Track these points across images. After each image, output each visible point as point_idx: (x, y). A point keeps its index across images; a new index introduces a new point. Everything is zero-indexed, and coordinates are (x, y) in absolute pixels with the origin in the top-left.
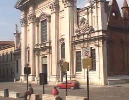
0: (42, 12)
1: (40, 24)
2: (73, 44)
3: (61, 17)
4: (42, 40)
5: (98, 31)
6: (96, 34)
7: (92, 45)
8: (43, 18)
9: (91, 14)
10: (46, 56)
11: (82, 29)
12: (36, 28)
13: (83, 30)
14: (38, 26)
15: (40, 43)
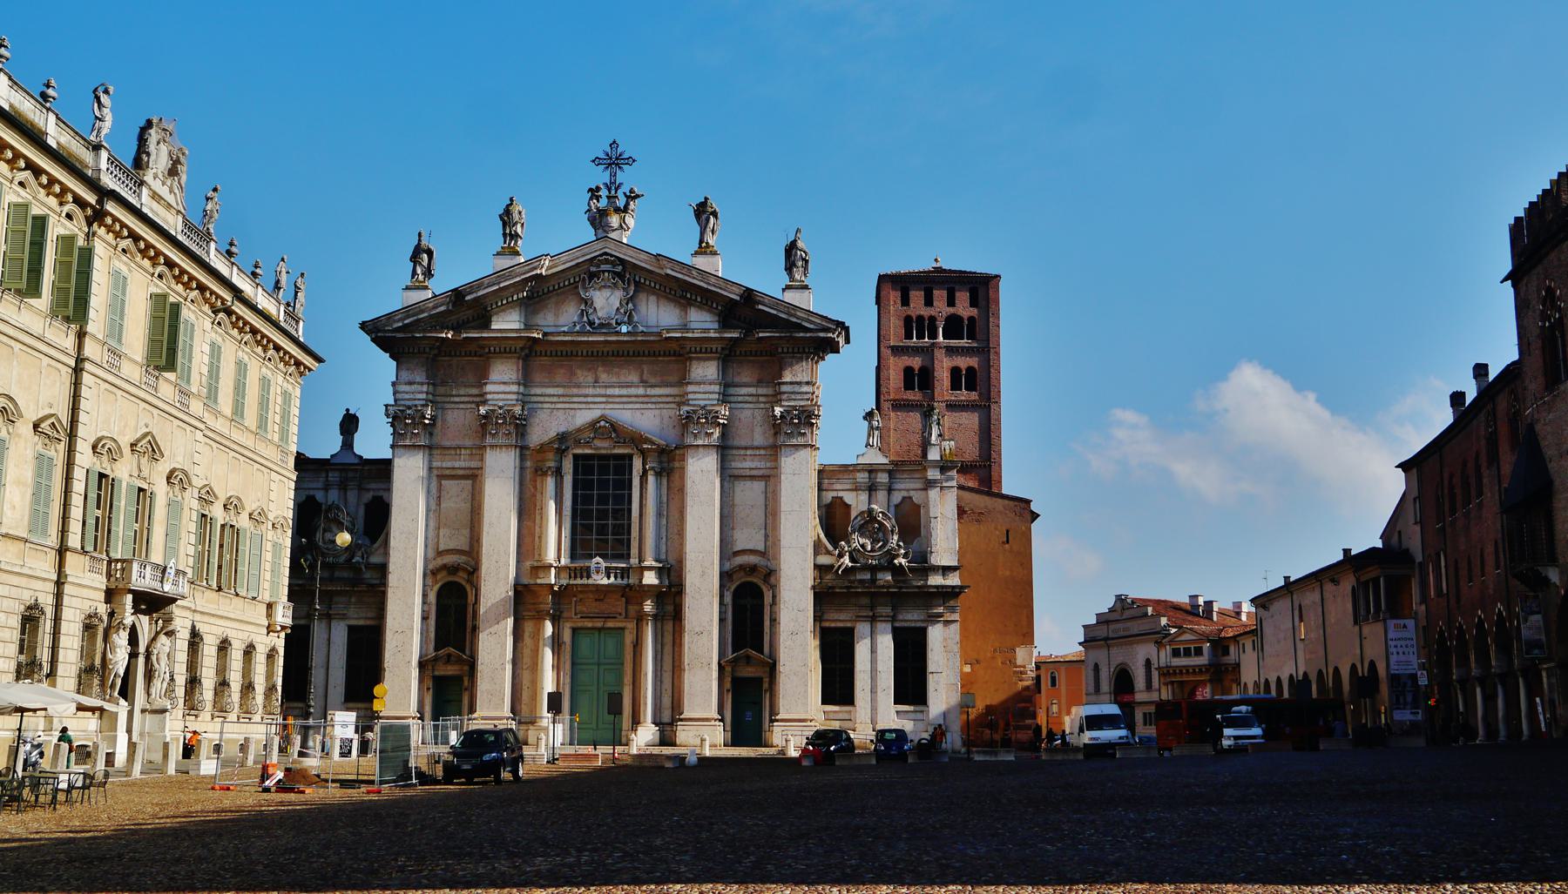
0: (601, 416)
1: (568, 466)
2: (823, 598)
3: (736, 472)
4: (580, 547)
5: (946, 570)
6: (936, 580)
7: (911, 617)
8: (598, 443)
9: (885, 493)
10: (610, 624)
11: (869, 548)
12: (550, 483)
13: (872, 551)
14: (558, 473)
15: (563, 561)
